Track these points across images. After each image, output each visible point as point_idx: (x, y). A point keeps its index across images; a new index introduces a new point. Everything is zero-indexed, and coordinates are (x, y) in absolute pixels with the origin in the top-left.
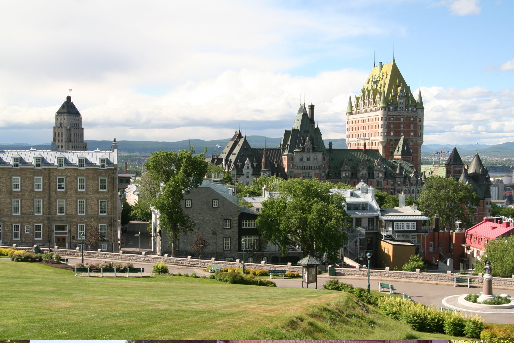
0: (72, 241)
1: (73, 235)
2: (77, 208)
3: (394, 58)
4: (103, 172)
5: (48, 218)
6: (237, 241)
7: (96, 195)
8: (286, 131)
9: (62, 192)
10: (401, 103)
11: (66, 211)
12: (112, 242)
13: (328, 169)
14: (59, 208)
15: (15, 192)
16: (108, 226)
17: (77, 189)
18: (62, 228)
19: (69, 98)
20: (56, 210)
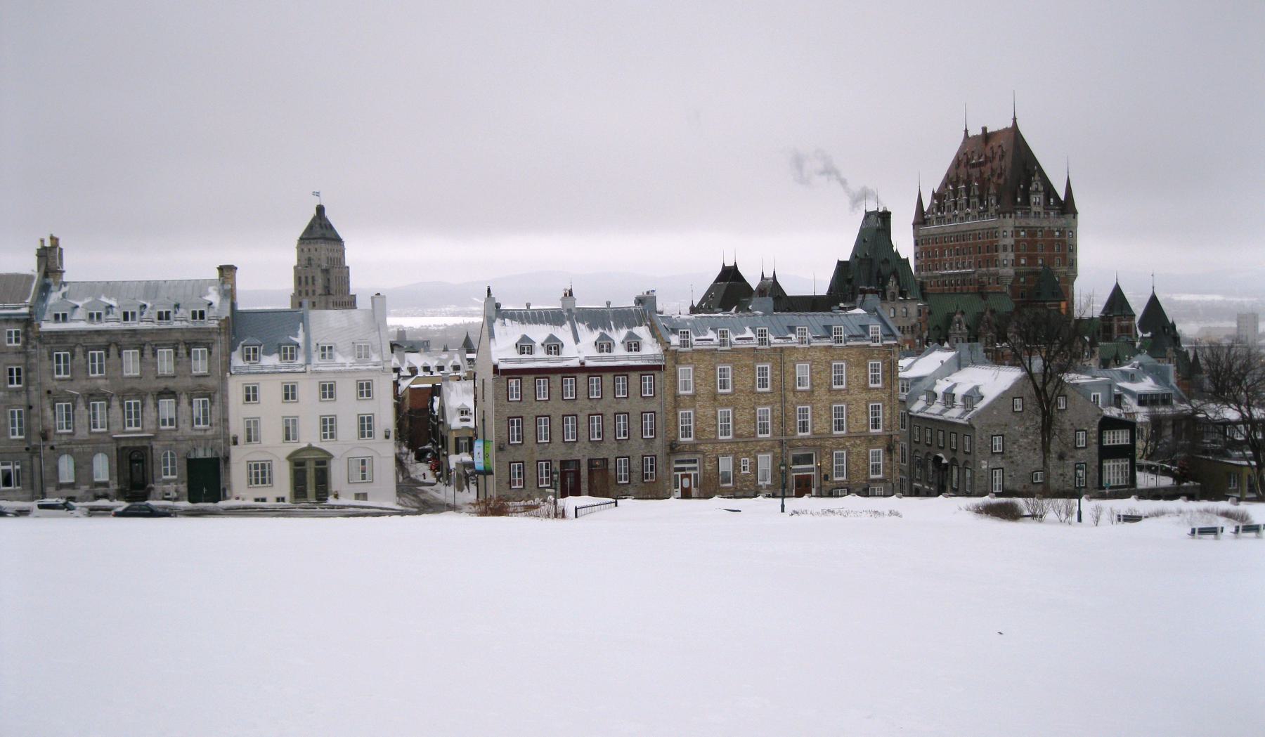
0: (823, 483)
1: (824, 472)
2: (831, 421)
3: (1015, 119)
4: (875, 352)
5: (781, 443)
6: (1097, 469)
7: (864, 394)
8: (840, 263)
9: (805, 391)
10: (1035, 203)
11: (813, 427)
12: (892, 482)
13: (927, 332)
14: (800, 422)
15: (722, 394)
16: (884, 453)
17: (830, 385)
18: (808, 459)
19: (320, 210)
20: (796, 426)
